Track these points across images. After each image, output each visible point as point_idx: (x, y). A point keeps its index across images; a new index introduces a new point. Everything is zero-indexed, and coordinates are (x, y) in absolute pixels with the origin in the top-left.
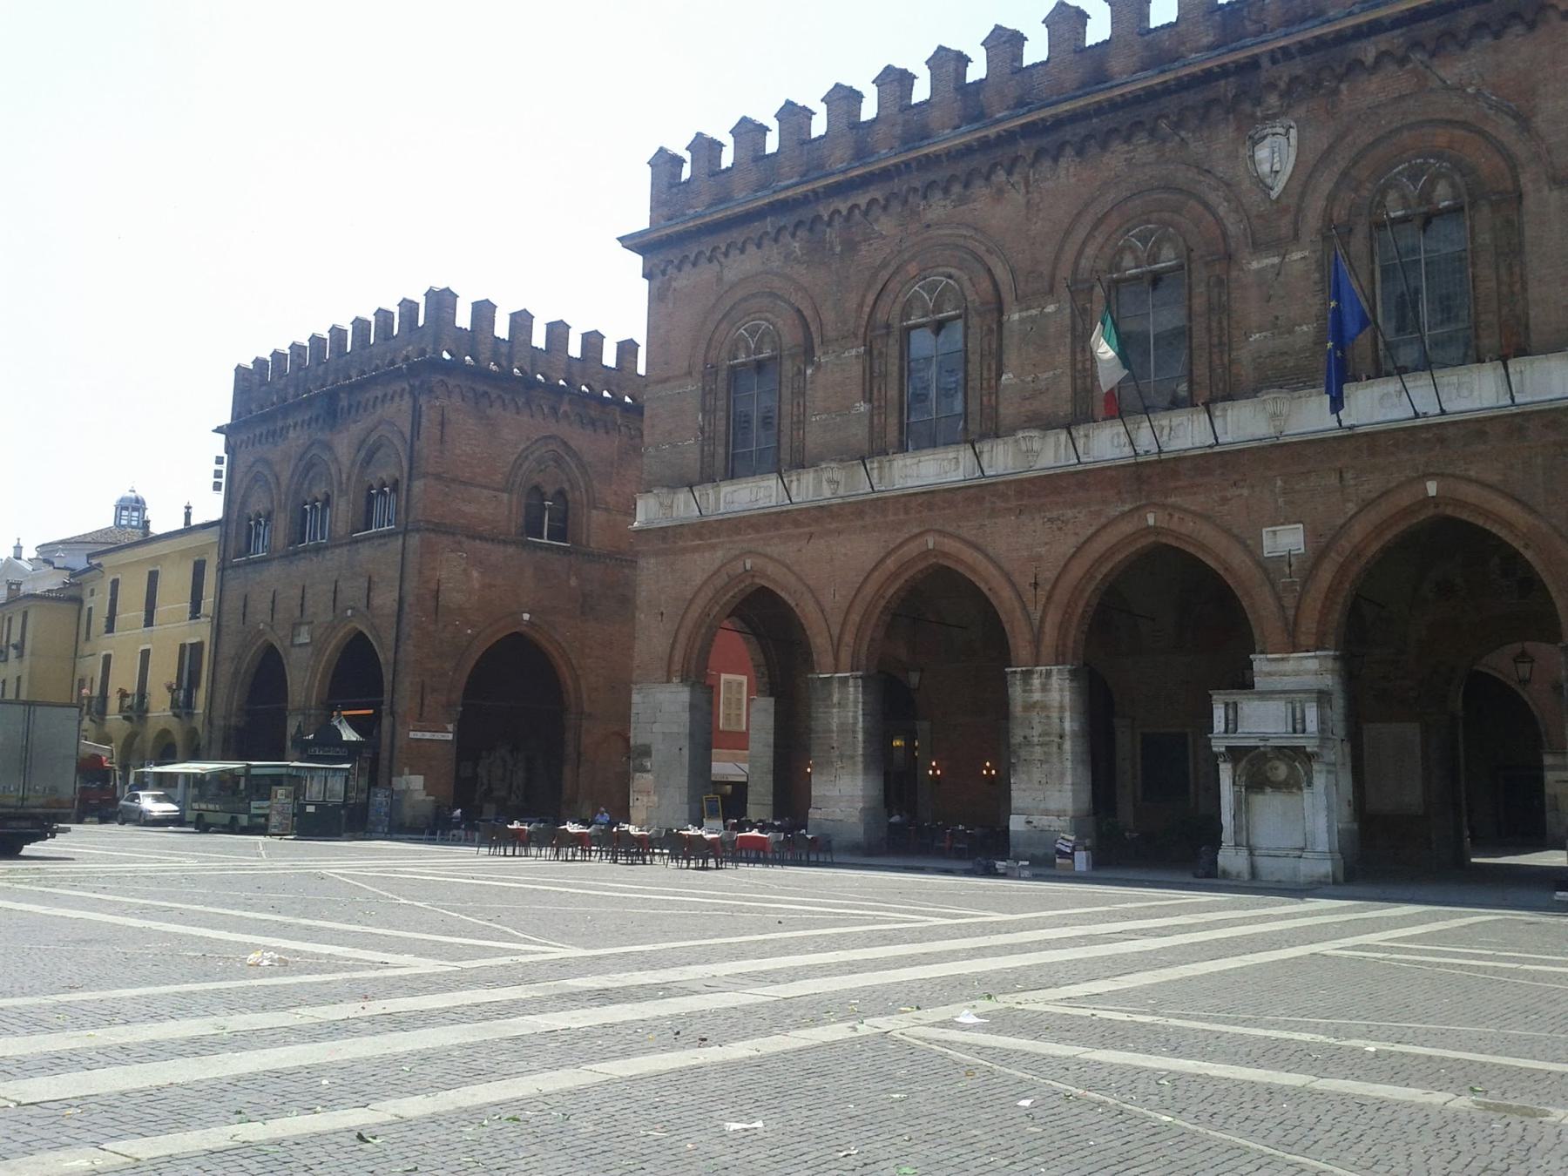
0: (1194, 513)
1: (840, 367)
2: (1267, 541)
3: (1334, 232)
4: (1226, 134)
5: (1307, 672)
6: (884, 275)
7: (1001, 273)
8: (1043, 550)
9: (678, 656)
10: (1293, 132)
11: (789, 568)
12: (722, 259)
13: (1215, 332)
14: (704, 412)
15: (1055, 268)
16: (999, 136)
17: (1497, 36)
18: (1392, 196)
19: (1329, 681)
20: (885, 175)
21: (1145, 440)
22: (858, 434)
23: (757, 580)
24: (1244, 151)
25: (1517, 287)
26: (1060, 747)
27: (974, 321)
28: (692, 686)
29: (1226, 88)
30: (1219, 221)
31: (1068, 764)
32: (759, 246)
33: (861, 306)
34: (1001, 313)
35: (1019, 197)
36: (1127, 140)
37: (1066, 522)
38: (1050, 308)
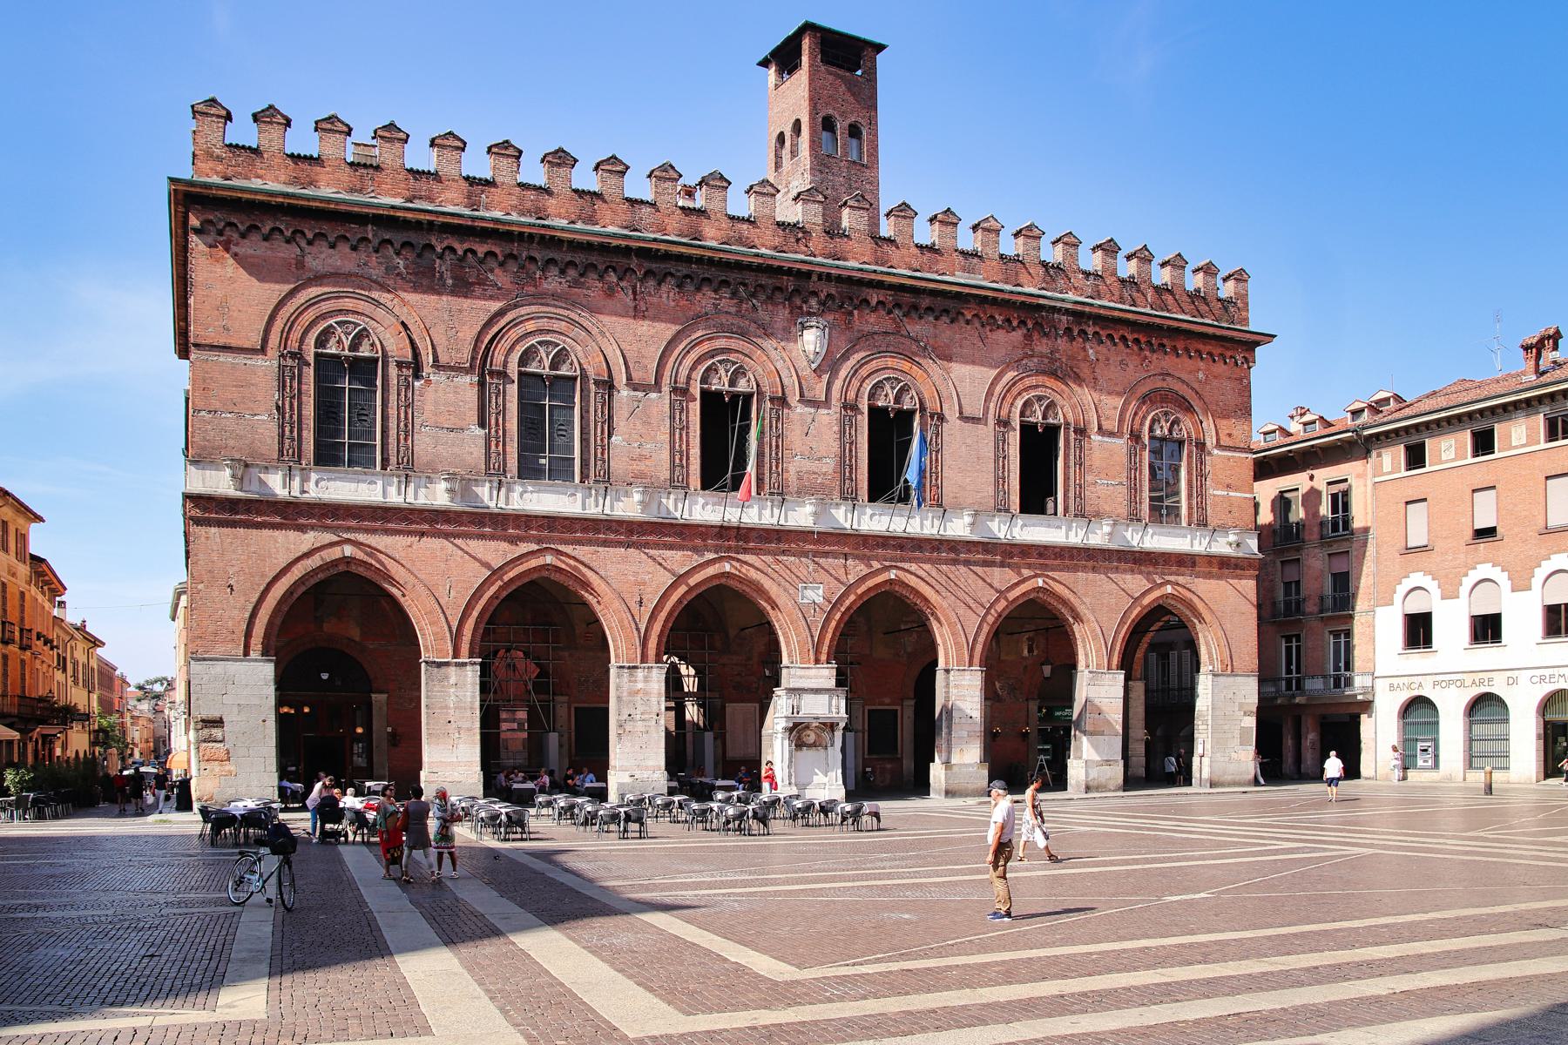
4: (783, 313)
16: (618, 247)
17: (937, 319)
36: (716, 291)
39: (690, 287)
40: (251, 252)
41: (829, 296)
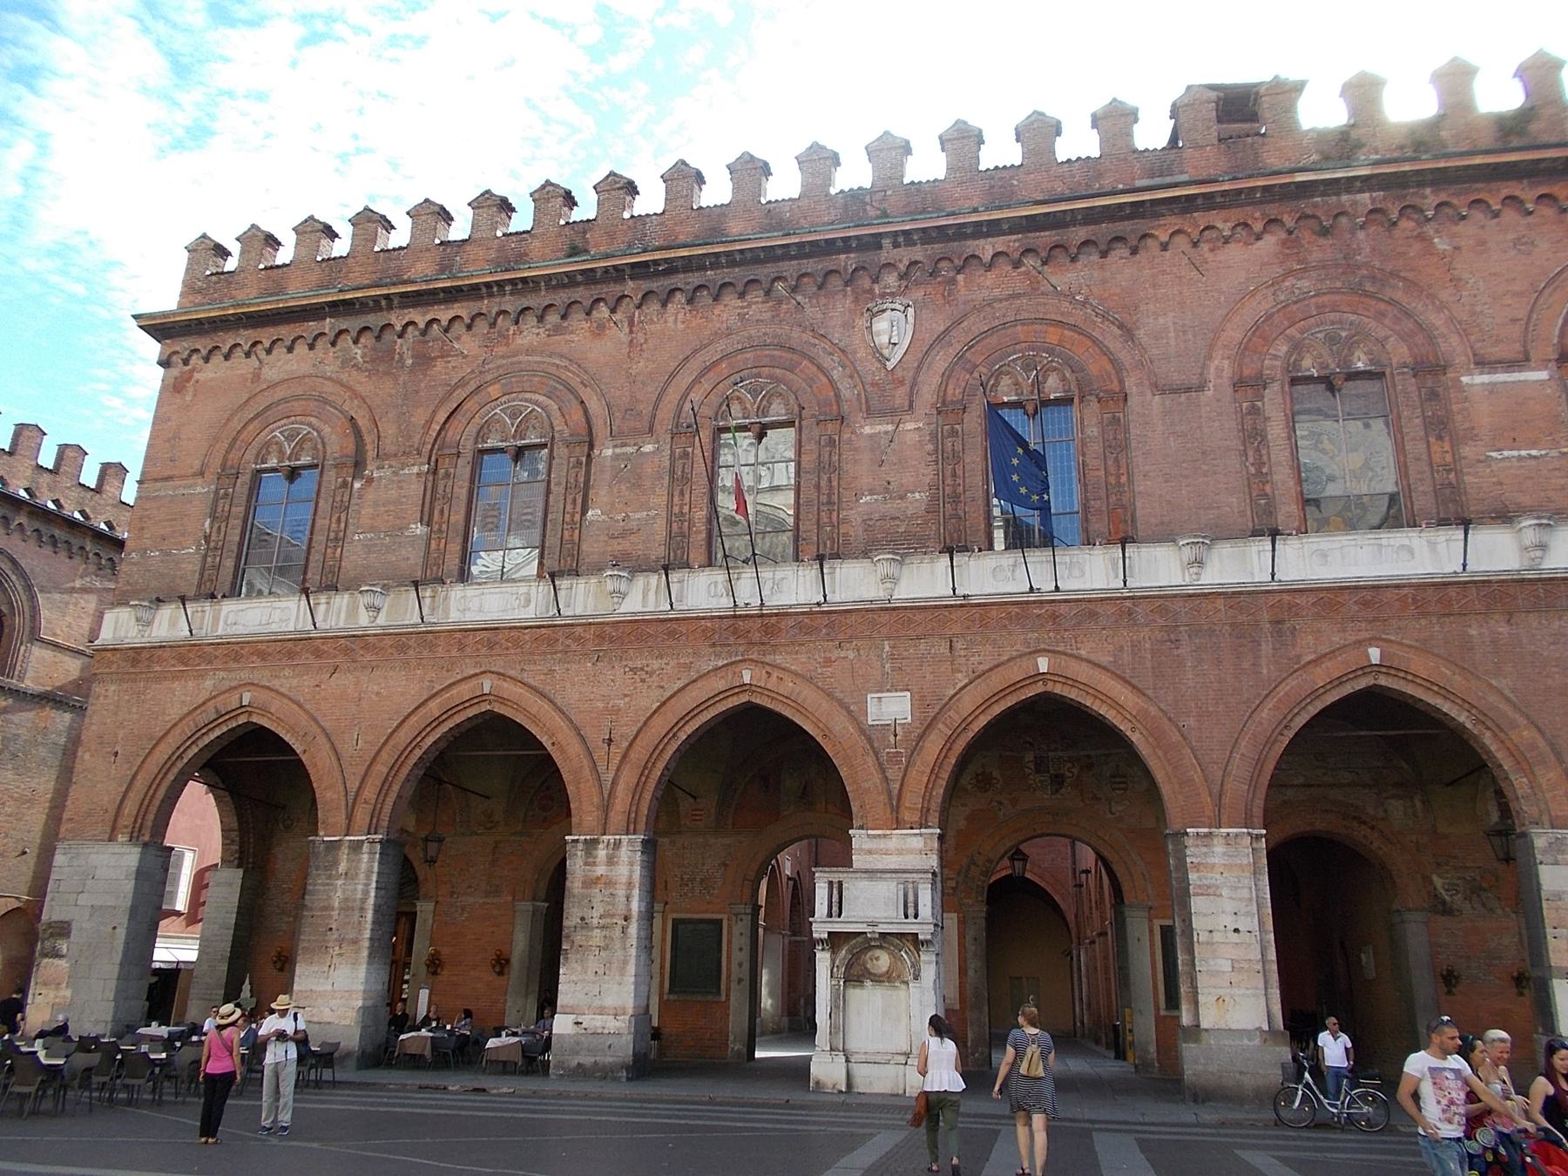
0: (796, 674)
1: (394, 487)
2: (872, 708)
3: (947, 409)
4: (842, 306)
5: (910, 851)
6: (460, 394)
7: (595, 406)
8: (621, 703)
9: (130, 808)
10: (911, 311)
11: (300, 706)
12: (262, 355)
13: (825, 490)
14: (214, 518)
15: (656, 408)
18: (1006, 381)
19: (933, 862)
20: (474, 292)
21: (747, 592)
22: (411, 558)
23: (254, 719)
24: (861, 322)
25: (1124, 479)
26: (624, 930)
27: (561, 451)
28: (145, 845)
29: (848, 261)
30: (831, 381)
31: (633, 951)
32: (311, 347)
33: (430, 422)
34: (591, 446)
35: (623, 335)
36: (742, 295)
37: (651, 674)
38: (648, 448)
39: (705, 297)
40: (211, 375)
41: (913, 263)
